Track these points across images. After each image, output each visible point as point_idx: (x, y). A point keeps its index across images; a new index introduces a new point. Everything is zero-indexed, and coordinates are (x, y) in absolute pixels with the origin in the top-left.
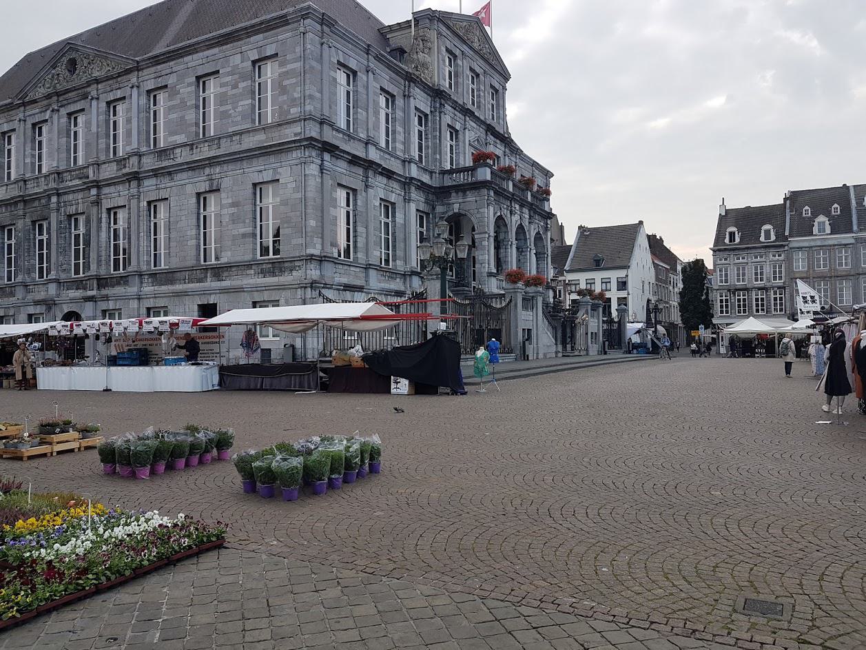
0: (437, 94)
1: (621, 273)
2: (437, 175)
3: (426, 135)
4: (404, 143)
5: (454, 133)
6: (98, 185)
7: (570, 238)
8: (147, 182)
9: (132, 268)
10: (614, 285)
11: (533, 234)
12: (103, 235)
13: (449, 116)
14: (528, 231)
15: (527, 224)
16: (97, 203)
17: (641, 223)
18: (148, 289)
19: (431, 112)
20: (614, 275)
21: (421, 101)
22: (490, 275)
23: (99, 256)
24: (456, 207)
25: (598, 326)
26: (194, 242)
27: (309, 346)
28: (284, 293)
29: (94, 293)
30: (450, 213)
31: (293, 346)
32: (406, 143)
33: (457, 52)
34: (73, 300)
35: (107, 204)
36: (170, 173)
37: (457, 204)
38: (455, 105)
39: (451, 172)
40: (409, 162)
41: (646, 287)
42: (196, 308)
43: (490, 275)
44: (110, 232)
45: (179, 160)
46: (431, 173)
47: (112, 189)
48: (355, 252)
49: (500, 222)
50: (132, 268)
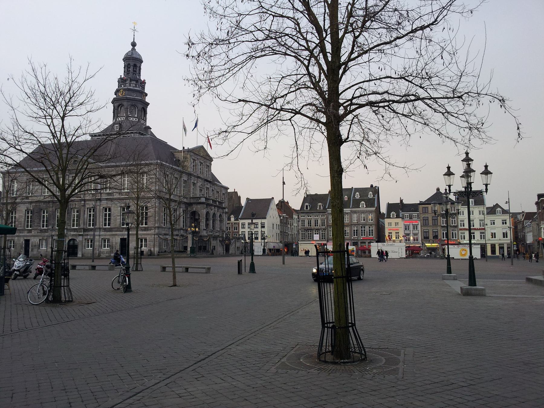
0: (190, 175)
1: (263, 221)
5: (194, 184)
6: (85, 200)
7: (243, 202)
8: (103, 202)
9: (97, 226)
10: (260, 226)
11: (218, 215)
12: (86, 216)
13: (193, 179)
16: (84, 206)
17: (273, 198)
18: (102, 233)
20: (259, 221)
21: (185, 178)
22: (204, 230)
23: (84, 222)
29: (82, 233)
31: (151, 250)
32: (180, 191)
33: (196, 159)
34: (73, 235)
35: (87, 206)
37: (194, 208)
38: (195, 176)
39: (193, 198)
41: (275, 226)
43: (204, 230)
45: (115, 197)
46: (187, 198)
47: (90, 202)
49: (208, 213)
50: (97, 226)
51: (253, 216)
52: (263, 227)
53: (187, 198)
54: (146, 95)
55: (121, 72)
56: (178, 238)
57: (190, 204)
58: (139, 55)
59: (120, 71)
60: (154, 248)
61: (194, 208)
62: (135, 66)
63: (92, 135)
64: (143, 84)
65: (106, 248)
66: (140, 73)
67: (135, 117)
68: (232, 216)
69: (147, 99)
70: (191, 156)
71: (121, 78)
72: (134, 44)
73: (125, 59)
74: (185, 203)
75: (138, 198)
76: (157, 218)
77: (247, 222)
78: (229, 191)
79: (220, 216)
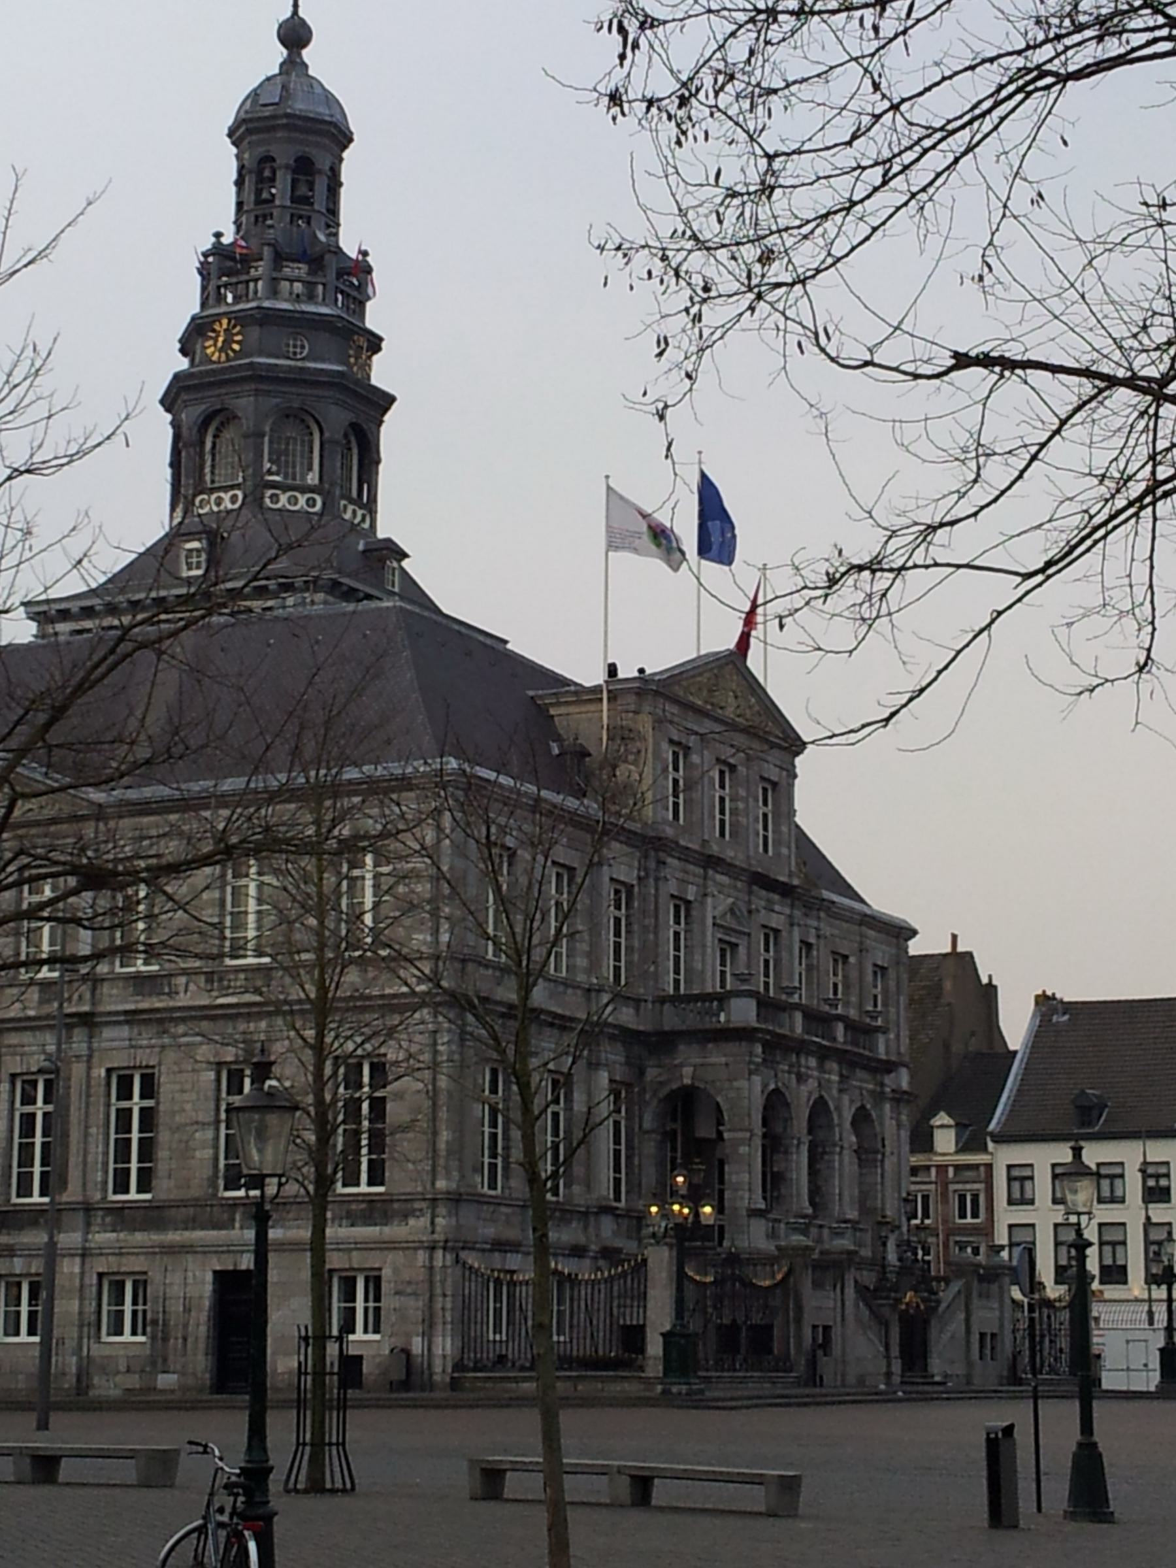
0: (652, 846)
2: (650, 1006)
3: (628, 924)
4: (589, 955)
5: (683, 906)
7: (1016, 1025)
8: (108, 1033)
9: (73, 1193)
10: (1133, 1185)
11: (848, 1115)
13: (676, 877)
14: (838, 1108)
15: (835, 1092)
18: (102, 1238)
19: (639, 878)
20: (1129, 1155)
21: (622, 865)
22: (754, 1213)
24: (687, 1071)
25: (1001, 1319)
26: (209, 1152)
27: (438, 1351)
28: (390, 1256)
30: (675, 1086)
31: (406, 1352)
33: (692, 741)
36: (161, 1021)
37: (687, 1066)
38: (685, 855)
39: (676, 999)
40: (599, 991)
42: (209, 1277)
43: (754, 1213)
44: (12, 1120)
45: (183, 1000)
46: (637, 1002)
47: (27, 1037)
48: (506, 1177)
49: (775, 1102)
50: (73, 1193)
51: (1086, 1119)
52: (1157, 1194)
53: (637, 1002)
54: (375, 343)
55: (215, 212)
56: (584, 1270)
57: (662, 1042)
58: (330, 99)
59: (210, 205)
60: (428, 1335)
61: (687, 1066)
62: (304, 167)
63: (44, 613)
64: (354, 278)
65: (127, 1337)
66: (333, 212)
67: (304, 489)
68: (942, 1118)
69: (382, 372)
70: (659, 723)
71: (218, 250)
72: (295, 35)
73: (241, 133)
74: (627, 1036)
75: (322, 1008)
76: (445, 1136)
77: (1044, 1157)
78: (915, 947)
79: (861, 1118)
